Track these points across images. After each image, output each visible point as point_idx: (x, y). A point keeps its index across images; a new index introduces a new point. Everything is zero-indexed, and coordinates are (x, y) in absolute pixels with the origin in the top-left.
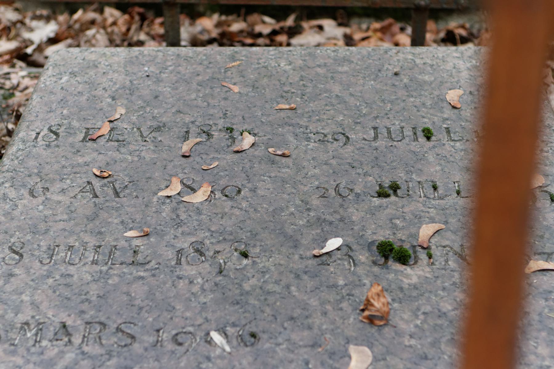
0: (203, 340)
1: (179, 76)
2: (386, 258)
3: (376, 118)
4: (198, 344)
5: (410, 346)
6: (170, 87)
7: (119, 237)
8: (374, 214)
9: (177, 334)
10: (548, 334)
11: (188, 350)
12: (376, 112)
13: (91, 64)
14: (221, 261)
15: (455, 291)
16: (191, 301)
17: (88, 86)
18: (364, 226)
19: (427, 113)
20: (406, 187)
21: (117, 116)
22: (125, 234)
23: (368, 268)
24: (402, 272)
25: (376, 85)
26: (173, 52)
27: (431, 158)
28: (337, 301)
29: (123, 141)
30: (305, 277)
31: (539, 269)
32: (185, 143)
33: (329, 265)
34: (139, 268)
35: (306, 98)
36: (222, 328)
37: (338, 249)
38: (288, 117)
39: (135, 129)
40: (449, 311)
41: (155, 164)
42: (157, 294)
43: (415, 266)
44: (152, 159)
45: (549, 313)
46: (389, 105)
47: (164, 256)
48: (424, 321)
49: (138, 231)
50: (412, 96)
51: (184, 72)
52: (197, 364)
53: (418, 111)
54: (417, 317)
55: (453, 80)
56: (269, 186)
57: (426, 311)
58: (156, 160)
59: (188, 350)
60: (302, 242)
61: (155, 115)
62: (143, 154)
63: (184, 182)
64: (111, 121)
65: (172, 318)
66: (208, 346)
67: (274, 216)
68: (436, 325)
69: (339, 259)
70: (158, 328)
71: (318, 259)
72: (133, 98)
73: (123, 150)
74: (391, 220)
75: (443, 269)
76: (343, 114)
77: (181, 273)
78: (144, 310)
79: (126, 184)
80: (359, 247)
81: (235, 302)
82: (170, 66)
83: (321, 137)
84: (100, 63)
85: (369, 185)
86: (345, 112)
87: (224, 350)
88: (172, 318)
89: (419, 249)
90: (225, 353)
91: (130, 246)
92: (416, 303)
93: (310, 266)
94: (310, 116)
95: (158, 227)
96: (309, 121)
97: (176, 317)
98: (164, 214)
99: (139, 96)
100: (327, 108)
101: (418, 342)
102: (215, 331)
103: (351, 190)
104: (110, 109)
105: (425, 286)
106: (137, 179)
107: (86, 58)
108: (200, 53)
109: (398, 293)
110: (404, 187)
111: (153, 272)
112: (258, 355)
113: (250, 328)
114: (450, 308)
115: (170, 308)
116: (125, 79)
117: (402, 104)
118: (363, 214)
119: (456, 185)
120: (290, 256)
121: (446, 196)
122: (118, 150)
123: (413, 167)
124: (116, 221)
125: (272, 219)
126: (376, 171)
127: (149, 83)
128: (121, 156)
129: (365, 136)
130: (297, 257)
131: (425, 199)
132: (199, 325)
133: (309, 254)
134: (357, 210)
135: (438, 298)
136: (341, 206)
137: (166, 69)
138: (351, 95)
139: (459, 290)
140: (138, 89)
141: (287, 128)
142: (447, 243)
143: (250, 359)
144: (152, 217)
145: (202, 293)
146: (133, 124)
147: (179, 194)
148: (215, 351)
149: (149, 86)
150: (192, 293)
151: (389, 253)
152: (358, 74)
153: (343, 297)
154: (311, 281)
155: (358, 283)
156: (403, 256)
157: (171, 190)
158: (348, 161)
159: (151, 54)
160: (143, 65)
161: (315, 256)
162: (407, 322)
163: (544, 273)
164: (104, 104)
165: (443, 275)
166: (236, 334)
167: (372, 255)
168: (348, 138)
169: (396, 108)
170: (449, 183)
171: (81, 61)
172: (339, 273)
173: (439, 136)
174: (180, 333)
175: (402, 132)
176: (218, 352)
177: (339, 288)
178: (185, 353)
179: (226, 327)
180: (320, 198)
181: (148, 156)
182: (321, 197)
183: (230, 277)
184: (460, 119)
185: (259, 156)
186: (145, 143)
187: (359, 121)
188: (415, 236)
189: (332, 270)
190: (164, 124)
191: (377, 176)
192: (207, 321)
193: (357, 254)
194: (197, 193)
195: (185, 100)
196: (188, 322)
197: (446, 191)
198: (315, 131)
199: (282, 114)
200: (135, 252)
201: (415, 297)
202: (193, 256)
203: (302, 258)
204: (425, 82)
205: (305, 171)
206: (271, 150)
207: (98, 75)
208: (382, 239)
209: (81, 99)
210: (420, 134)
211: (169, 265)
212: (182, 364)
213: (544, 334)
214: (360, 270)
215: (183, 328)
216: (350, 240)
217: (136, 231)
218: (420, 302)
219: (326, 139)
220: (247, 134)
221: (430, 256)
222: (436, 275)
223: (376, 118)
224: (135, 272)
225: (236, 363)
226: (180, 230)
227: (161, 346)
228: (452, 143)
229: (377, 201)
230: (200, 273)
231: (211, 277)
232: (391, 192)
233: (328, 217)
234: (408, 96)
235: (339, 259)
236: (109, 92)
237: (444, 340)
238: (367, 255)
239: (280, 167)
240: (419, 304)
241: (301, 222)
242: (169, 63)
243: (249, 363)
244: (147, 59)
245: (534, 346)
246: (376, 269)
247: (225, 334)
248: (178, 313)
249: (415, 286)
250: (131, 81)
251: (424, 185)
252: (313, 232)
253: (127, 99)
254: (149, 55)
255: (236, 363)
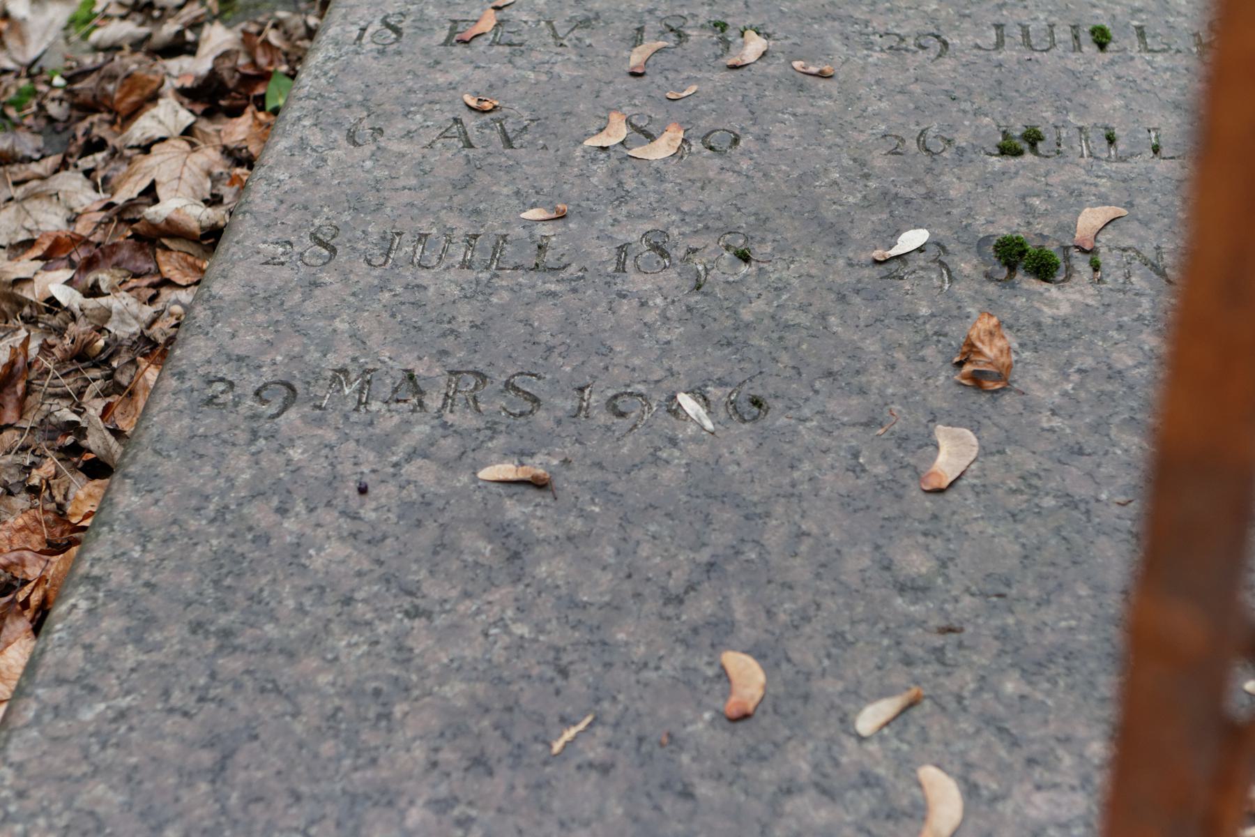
2: (1012, 268)
5: (1052, 430)
9: (615, 397)
11: (635, 426)
14: (700, 268)
15: (1141, 331)
16: (643, 337)
18: (970, 209)
22: (523, 215)
23: (977, 286)
24: (1041, 294)
27: (1105, 83)
28: (916, 343)
29: (521, 45)
30: (857, 300)
32: (635, 50)
33: (901, 278)
34: (548, 276)
37: (920, 250)
39: (543, 23)
40: (1129, 368)
42: (581, 324)
44: (574, 78)
48: (1080, 386)
54: (1066, 377)
56: (794, 131)
57: (1083, 367)
58: (580, 80)
62: (557, 69)
63: (634, 121)
64: (497, 8)
65: (606, 368)
68: (1103, 392)
69: (922, 268)
70: (582, 384)
71: (881, 268)
73: (519, 61)
74: (1023, 197)
75: (1119, 290)
78: (557, 351)
80: (960, 247)
81: (724, 342)
85: (983, 132)
87: (703, 428)
88: (606, 368)
89: (1074, 253)
91: (531, 236)
92: (1066, 353)
95: (584, 204)
96: (871, 12)
98: (594, 180)
110: (1050, 137)
115: (604, 350)
119: (1153, 134)
121: (1132, 155)
122: (510, 62)
124: (505, 191)
126: (998, 106)
128: (515, 72)
129: (979, 42)
130: (841, 262)
131: (1091, 160)
132: (657, 382)
133: (864, 257)
134: (959, 178)
136: (929, 170)
139: (1149, 330)
141: (829, 24)
143: (751, 444)
144: (573, 184)
146: (540, 13)
147: (622, 143)
150: (645, 324)
153: (927, 338)
154: (867, 307)
155: (955, 313)
157: (608, 135)
161: (876, 262)
162: (1048, 386)
165: (1120, 303)
166: (725, 399)
167: (985, 263)
168: (945, 44)
172: (920, 294)
174: (622, 394)
175: (1052, 34)
176: (691, 429)
177: (921, 321)
178: (631, 430)
181: (566, 73)
183: (715, 296)
184: (1167, 10)
185: (774, 77)
186: (560, 49)
187: (967, 12)
188: (1070, 229)
189: (908, 287)
190: (597, 14)
191: (998, 117)
192: (672, 375)
193: (956, 259)
197: (1132, 147)
198: (882, 30)
200: (540, 247)
201: (1063, 341)
202: (648, 257)
203: (851, 265)
205: (862, 104)
206: (797, 64)
208: (1005, 232)
210: (1085, 37)
214: (960, 289)
215: (628, 386)
216: (942, 233)
219: (904, 45)
220: (753, 33)
222: (1107, 301)
223: (1001, 6)
226: (624, 209)
228: (1148, 57)
229: (997, 163)
231: (680, 295)
233: (902, 191)
235: (922, 268)
238: (975, 262)
239: (813, 97)
240: (1071, 354)
241: (851, 200)
246: (991, 288)
247: (705, 399)
251: (1091, 134)
252: (874, 218)
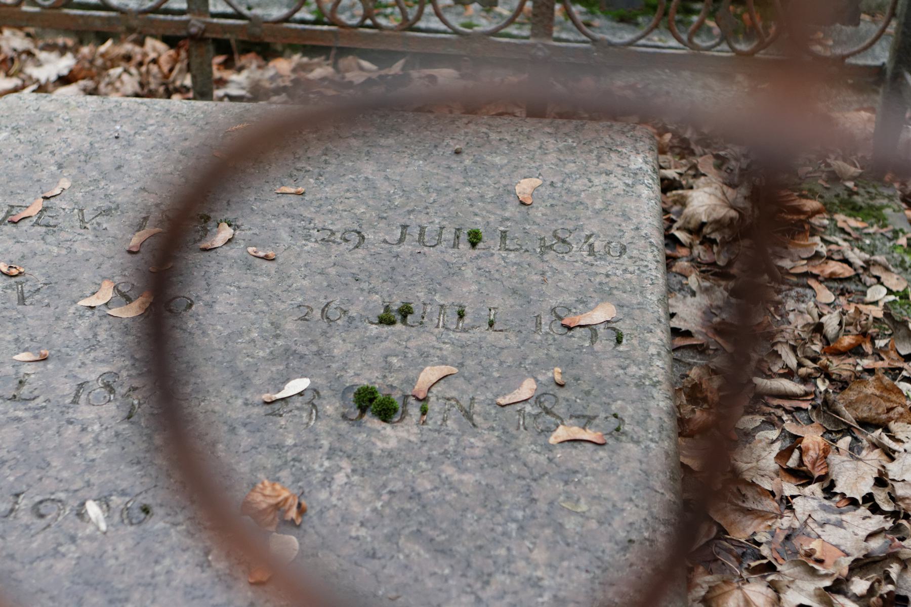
0: (75, 512)
1: (159, 139)
2: (363, 410)
3: (410, 212)
4: (65, 518)
5: (357, 538)
6: (142, 154)
7: (6, 360)
8: (365, 347)
9: (41, 502)
10: (554, 532)
11: (49, 526)
12: (412, 204)
13: (45, 117)
14: (136, 402)
15: (443, 463)
16: (75, 455)
17: (30, 148)
18: (346, 364)
19: (484, 209)
20: (422, 312)
21: (57, 191)
22: (16, 357)
23: (333, 424)
24: (379, 431)
25: (425, 166)
26: (161, 106)
27: (468, 273)
28: (276, 467)
29: (55, 226)
30: (243, 431)
31: (569, 438)
32: (137, 234)
33: (281, 416)
34: (21, 406)
35: (322, 179)
36: (105, 497)
37: (300, 394)
38: (291, 205)
39: (76, 211)
40: (426, 491)
41: (87, 260)
42: (32, 443)
43: (399, 424)
44: (86, 253)
45: (564, 502)
46: (435, 195)
47: (57, 391)
48: (388, 504)
49: (33, 354)
50: (470, 184)
51: (166, 135)
52: (55, 545)
53: (471, 205)
54: (379, 496)
55: (534, 165)
56: (235, 300)
57: (394, 489)
58: (90, 255)
59: (49, 526)
60: (254, 381)
61: (109, 192)
62: (76, 246)
63: (120, 288)
64: (45, 198)
65: (41, 479)
66: (78, 521)
67: (226, 343)
68: (402, 509)
69: (298, 409)
70: (18, 491)
71: (268, 407)
72: (88, 166)
73: (50, 239)
74: (386, 357)
75: (436, 430)
76: (367, 204)
77: (74, 416)
78: (8, 464)
79: (40, 286)
80: (330, 393)
81: (135, 461)
82: (152, 125)
83: (326, 235)
84: (58, 116)
85: (371, 306)
86: (371, 203)
87: (98, 529)
88: (41, 479)
89: (412, 400)
90: (98, 533)
91: (17, 373)
92: (384, 478)
93: (254, 416)
94: (321, 205)
95: (63, 350)
96: (317, 212)
97: (48, 477)
98: (77, 332)
99: (96, 165)
100: (348, 195)
101: (370, 532)
102: (95, 500)
103: (345, 312)
104: (50, 180)
105: (404, 453)
106: (56, 280)
107: (41, 108)
108: (199, 108)
109: (364, 460)
110: (418, 312)
111: (37, 412)
112: (143, 538)
113: (144, 498)
114: (429, 486)
115: (43, 465)
116: (84, 140)
117: (452, 195)
118: (349, 346)
119: (493, 312)
120: (231, 401)
121: (473, 327)
122: (43, 239)
123: (440, 284)
124: (9, 338)
125: (223, 347)
126: (388, 287)
127: (116, 147)
128: (44, 247)
129: (387, 238)
130: (240, 402)
131: (442, 330)
132: (76, 491)
133: (257, 399)
134: (344, 340)
135: (417, 472)
136: (324, 333)
137: (145, 129)
138: (387, 178)
139: (449, 462)
140: (97, 154)
141: (284, 219)
142: (454, 394)
143: (130, 542)
144: (60, 334)
145: (94, 445)
146: (76, 203)
147: (106, 304)
148: (85, 528)
149: (114, 151)
150: (81, 445)
151: (368, 403)
152: (405, 150)
153: (286, 463)
154: (248, 437)
155: (312, 444)
156: (384, 409)
157: (98, 298)
158: (353, 271)
159: (131, 107)
160: (116, 121)
161: (266, 403)
162: (364, 503)
163: (575, 444)
164: (44, 173)
165: (434, 440)
166: (122, 506)
167: (344, 406)
168: (363, 238)
169: (443, 200)
170: (483, 310)
171: (33, 112)
172: (291, 428)
173: (490, 242)
174: (46, 500)
175: (440, 234)
176: (90, 530)
177: (285, 449)
178: (45, 529)
179: (111, 495)
180: (299, 322)
181: (81, 248)
182: (302, 319)
183: (140, 425)
184: (527, 220)
185: (232, 258)
186: (82, 231)
187: (385, 215)
188: (411, 382)
189: (283, 423)
190: (118, 205)
191: (385, 295)
192: (89, 486)
193: (324, 402)
194: (132, 304)
195: (156, 174)
196: (61, 485)
197: (475, 321)
198: (320, 226)
199: (284, 201)
200: (21, 382)
201: (385, 468)
202: (98, 393)
203: (246, 404)
204: (494, 165)
205: (290, 282)
206: (251, 249)
207: (49, 133)
208: (365, 383)
209: (16, 165)
210: (464, 237)
211: (61, 403)
212: (35, 545)
213: (548, 532)
214: (321, 426)
215: (52, 493)
216: (320, 381)
217: (30, 354)
218: (390, 476)
219: (332, 238)
220: (226, 225)
221: (424, 412)
222: (424, 438)
223: (410, 212)
224: (11, 410)
225: (109, 548)
226: (93, 355)
227: (15, 517)
228: (504, 254)
229: (374, 329)
230: (100, 418)
231: (113, 424)
232: (399, 317)
233: (301, 349)
234: (464, 183)
235: (298, 409)
236: (57, 158)
237: (407, 531)
238: (338, 405)
239: (256, 275)
240: (387, 480)
241: (261, 354)
242: (151, 122)
243: (126, 549)
244: (123, 113)
245: (529, 548)
246: (344, 426)
247: (108, 506)
248: (53, 472)
249: (389, 453)
250: (91, 144)
251: (448, 310)
252: (274, 369)
253: (79, 167)
254: (128, 108)
255: (109, 548)
